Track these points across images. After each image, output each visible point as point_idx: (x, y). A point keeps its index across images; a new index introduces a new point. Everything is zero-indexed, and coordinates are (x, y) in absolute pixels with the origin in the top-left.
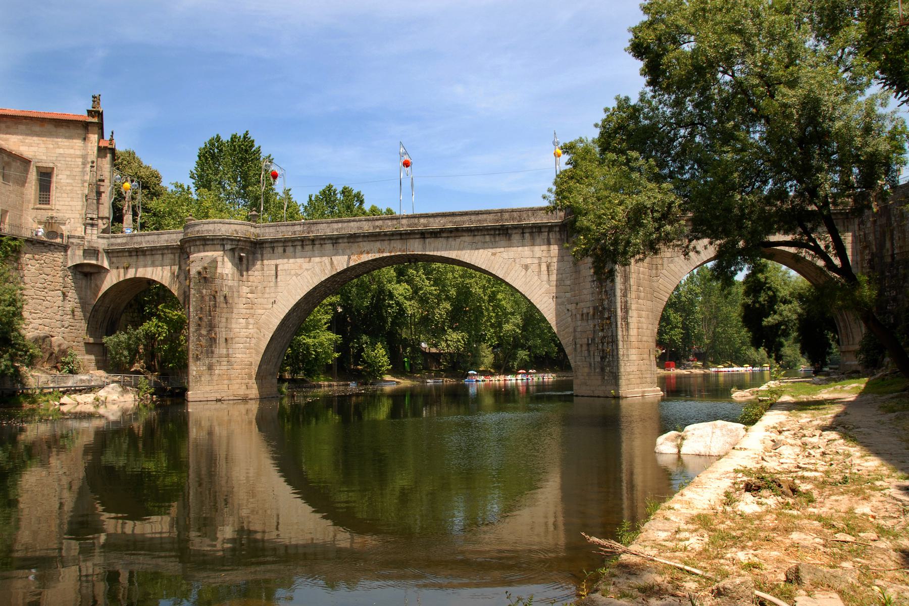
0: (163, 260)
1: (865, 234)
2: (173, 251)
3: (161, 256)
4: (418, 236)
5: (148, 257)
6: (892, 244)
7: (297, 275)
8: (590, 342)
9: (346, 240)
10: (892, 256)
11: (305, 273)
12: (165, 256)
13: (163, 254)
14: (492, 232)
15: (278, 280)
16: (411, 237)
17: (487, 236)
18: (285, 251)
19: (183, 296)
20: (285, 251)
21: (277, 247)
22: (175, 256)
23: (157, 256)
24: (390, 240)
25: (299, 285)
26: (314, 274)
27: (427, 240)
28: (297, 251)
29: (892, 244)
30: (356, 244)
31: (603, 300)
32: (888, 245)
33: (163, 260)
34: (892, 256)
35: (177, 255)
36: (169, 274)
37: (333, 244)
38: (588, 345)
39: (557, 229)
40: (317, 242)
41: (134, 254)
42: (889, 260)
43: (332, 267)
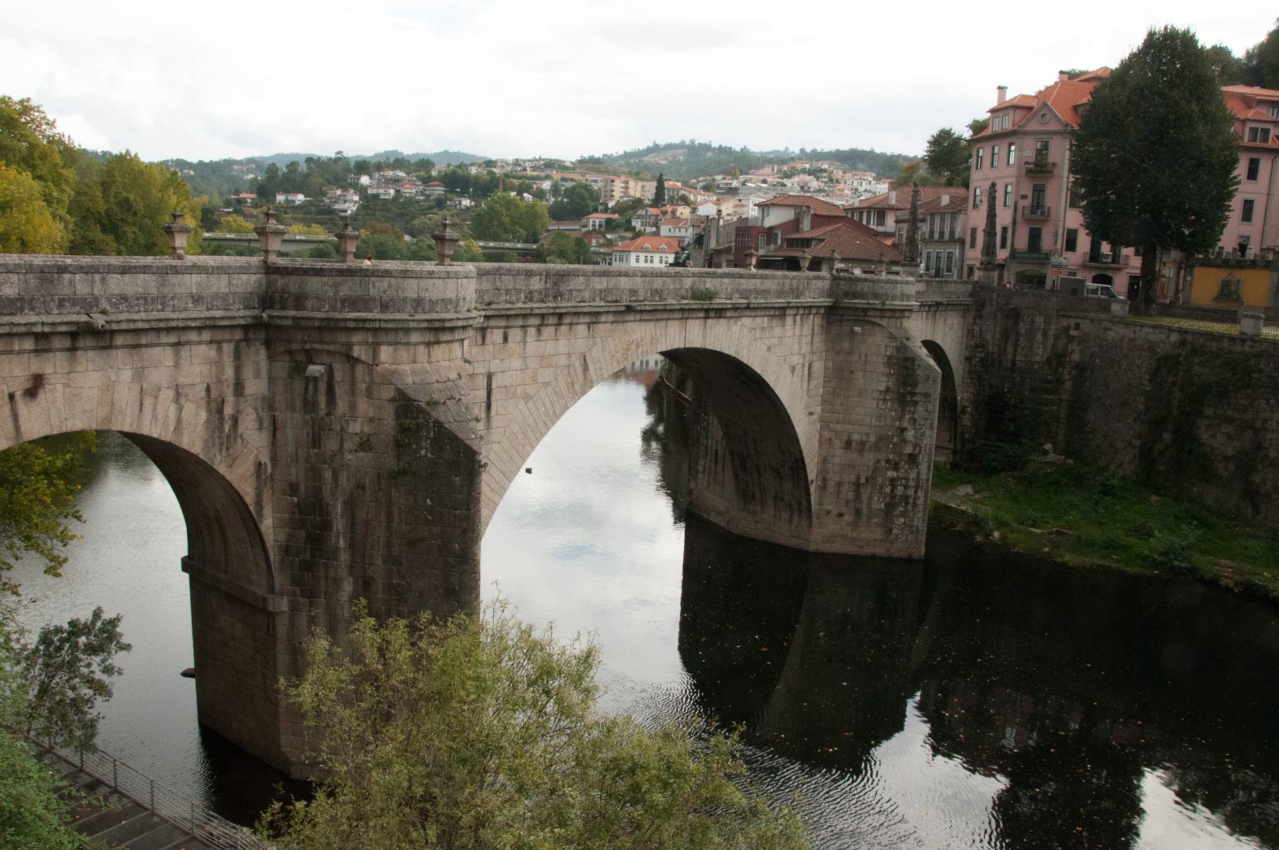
0: (177, 365)
1: (981, 329)
2: (219, 335)
3: (169, 350)
4: (702, 315)
5: (120, 355)
6: (1015, 349)
7: (527, 397)
8: (863, 480)
9: (611, 318)
10: (1014, 361)
11: (542, 393)
12: (185, 352)
13: (178, 344)
14: (772, 312)
15: (493, 413)
16: (694, 315)
17: (766, 318)
18: (506, 339)
19: (253, 481)
20: (506, 339)
21: (492, 328)
22: (219, 349)
23: (157, 350)
24: (668, 319)
25: (531, 422)
26: (556, 393)
27: (710, 322)
28: (529, 339)
29: (1015, 349)
30: (621, 326)
31: (903, 430)
32: (1010, 349)
33: (177, 365)
34: (1014, 361)
35: (228, 348)
36: (203, 415)
37: (589, 324)
38: (857, 485)
39: (822, 311)
40: (567, 320)
41: (57, 343)
42: (1009, 365)
43: (585, 378)
